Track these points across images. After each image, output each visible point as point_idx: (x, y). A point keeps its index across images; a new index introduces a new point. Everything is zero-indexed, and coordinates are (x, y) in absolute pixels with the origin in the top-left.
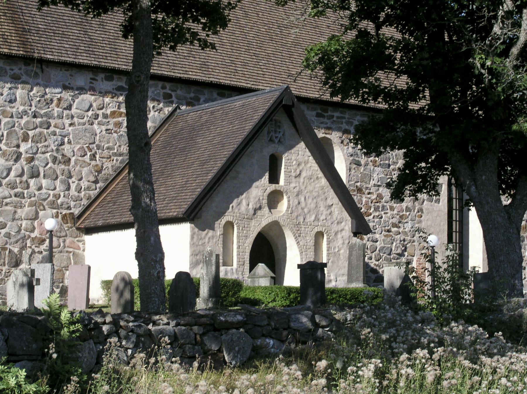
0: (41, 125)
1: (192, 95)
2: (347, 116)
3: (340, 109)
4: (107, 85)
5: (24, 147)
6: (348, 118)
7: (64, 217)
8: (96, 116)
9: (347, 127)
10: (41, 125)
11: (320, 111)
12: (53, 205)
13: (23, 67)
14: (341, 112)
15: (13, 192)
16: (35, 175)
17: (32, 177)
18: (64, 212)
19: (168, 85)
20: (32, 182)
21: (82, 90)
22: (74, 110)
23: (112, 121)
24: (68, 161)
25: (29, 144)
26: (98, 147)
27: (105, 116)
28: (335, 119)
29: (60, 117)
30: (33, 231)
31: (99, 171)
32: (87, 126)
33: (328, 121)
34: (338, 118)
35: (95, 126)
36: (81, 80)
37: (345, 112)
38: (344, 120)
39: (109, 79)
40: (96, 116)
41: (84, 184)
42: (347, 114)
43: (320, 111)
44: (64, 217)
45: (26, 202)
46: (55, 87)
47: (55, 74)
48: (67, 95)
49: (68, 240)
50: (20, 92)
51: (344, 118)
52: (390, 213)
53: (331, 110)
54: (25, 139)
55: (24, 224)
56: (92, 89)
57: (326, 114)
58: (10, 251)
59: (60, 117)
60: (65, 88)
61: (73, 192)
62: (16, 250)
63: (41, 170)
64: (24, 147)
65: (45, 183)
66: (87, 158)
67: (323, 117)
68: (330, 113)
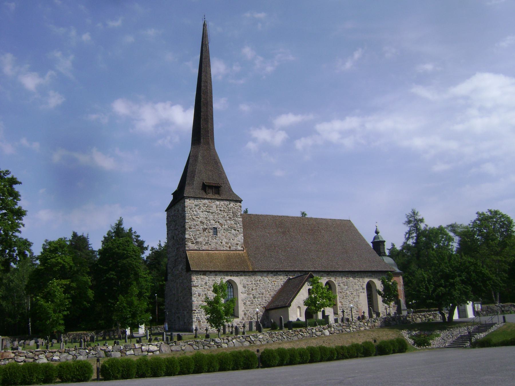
1: (293, 274)
2: (335, 274)
4: (272, 275)
11: (327, 274)
13: (251, 273)
15: (249, 303)
16: (254, 298)
18: (263, 306)
19: (287, 273)
26: (270, 290)
29: (260, 284)
32: (267, 285)
34: (333, 275)
36: (265, 274)
43: (327, 274)
52: (350, 297)
58: (251, 317)
66: (267, 293)
67: (329, 275)
68: (330, 274)
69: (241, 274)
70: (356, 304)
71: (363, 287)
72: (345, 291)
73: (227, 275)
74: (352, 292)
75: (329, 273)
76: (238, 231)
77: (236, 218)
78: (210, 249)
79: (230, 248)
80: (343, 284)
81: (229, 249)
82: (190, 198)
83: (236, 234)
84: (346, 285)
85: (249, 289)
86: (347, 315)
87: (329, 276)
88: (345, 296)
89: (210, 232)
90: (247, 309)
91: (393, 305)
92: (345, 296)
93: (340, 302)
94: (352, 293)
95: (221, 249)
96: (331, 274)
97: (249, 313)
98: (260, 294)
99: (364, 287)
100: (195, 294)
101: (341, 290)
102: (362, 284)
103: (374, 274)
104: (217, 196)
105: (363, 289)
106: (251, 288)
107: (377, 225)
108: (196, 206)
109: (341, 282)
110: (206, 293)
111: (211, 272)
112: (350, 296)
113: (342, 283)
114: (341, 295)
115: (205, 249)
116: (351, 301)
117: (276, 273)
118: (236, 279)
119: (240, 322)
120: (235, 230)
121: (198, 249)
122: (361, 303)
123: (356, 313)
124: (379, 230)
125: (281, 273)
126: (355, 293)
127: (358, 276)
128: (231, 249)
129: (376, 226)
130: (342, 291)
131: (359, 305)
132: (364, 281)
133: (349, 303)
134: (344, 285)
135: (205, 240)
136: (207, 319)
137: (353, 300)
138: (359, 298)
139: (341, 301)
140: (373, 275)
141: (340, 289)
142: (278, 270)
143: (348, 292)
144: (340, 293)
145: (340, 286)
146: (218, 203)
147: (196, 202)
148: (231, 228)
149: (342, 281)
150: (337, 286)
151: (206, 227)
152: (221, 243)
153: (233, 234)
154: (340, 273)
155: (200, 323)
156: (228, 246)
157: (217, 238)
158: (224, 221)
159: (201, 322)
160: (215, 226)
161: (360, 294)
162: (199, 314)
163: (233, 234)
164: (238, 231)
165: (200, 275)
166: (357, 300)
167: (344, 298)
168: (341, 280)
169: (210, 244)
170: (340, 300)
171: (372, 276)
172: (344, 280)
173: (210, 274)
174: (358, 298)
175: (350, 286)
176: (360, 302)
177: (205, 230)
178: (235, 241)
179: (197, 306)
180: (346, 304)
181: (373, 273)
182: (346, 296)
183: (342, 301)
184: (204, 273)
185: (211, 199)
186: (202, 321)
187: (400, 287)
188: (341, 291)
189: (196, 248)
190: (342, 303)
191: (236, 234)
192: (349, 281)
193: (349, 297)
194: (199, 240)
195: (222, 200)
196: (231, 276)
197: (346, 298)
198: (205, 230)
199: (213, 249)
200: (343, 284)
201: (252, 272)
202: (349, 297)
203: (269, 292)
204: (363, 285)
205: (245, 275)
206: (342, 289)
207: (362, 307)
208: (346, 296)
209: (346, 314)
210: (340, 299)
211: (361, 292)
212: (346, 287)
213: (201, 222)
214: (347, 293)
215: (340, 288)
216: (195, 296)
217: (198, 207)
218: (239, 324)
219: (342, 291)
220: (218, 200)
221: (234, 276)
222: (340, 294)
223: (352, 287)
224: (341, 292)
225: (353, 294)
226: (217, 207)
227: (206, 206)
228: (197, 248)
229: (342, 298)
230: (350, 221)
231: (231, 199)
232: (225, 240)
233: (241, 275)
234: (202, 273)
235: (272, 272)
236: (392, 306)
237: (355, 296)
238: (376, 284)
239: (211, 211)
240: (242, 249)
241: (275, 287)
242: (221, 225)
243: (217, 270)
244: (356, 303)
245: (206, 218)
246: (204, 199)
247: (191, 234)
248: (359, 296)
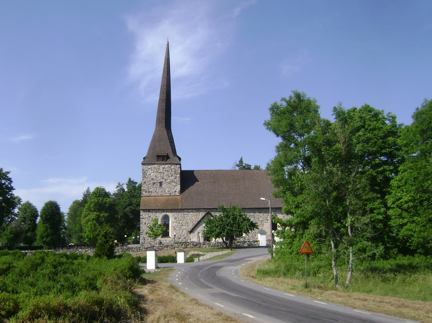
0: (183, 218)
4: (195, 211)
5: (181, 222)
7: (188, 231)
8: (193, 216)
10: (183, 218)
12: (186, 230)
16: (182, 225)
17: (182, 226)
20: (182, 227)
21: (190, 212)
22: (189, 215)
23: (196, 216)
24: (188, 223)
25: (181, 221)
27: (194, 216)
29: (187, 217)
30: (182, 234)
31: (194, 224)
35: (193, 217)
36: (190, 211)
39: (195, 210)
40: (193, 216)
41: (191, 226)
44: (188, 231)
45: (181, 230)
46: (186, 212)
47: (185, 210)
48: (188, 213)
49: (188, 235)
50: (180, 214)
54: (181, 220)
55: (181, 233)
56: (192, 212)
59: (187, 217)
60: (187, 212)
61: (189, 227)
62: (179, 237)
63: (184, 225)
64: (181, 222)
65: (184, 227)
66: (191, 222)
69: (173, 210)
71: (268, 219)
73: (164, 212)
76: (177, 183)
77: (175, 175)
78: (157, 195)
79: (170, 194)
81: (169, 195)
82: (146, 165)
83: (176, 186)
85: (178, 220)
89: (158, 185)
90: (177, 232)
95: (164, 195)
97: (178, 235)
98: (186, 223)
100: (143, 223)
102: (266, 217)
103: (278, 210)
104: (163, 162)
105: (268, 220)
106: (180, 220)
108: (149, 169)
110: (149, 222)
111: (153, 210)
115: (154, 195)
117: (198, 210)
118: (170, 215)
119: (171, 240)
120: (175, 183)
121: (149, 196)
125: (202, 210)
127: (264, 211)
128: (172, 195)
135: (153, 190)
136: (161, 237)
140: (277, 211)
142: (199, 208)
146: (163, 166)
147: (149, 167)
148: (172, 182)
151: (155, 181)
152: (165, 191)
153: (174, 186)
155: (145, 241)
156: (169, 193)
157: (162, 189)
158: (168, 178)
159: (146, 240)
160: (161, 181)
162: (144, 235)
163: (174, 186)
164: (177, 183)
165: (146, 211)
169: (157, 192)
171: (276, 211)
173: (153, 211)
177: (154, 183)
178: (174, 190)
179: (143, 230)
184: (149, 211)
185: (159, 164)
186: (146, 239)
189: (148, 195)
191: (176, 186)
194: (150, 190)
195: (167, 164)
196: (166, 212)
198: (154, 183)
199: (159, 195)
201: (181, 209)
203: (192, 222)
204: (267, 217)
205: (176, 212)
209: (251, 237)
211: (266, 222)
213: (153, 179)
216: (142, 224)
217: (151, 170)
218: (171, 242)
220: (164, 164)
221: (168, 212)
226: (163, 169)
227: (156, 168)
228: (149, 195)
231: (173, 163)
232: (168, 189)
233: (174, 212)
234: (147, 211)
235: (195, 209)
239: (159, 172)
240: (179, 194)
241: (197, 219)
242: (165, 180)
243: (157, 208)
245: (156, 176)
246: (155, 164)
247: (146, 186)
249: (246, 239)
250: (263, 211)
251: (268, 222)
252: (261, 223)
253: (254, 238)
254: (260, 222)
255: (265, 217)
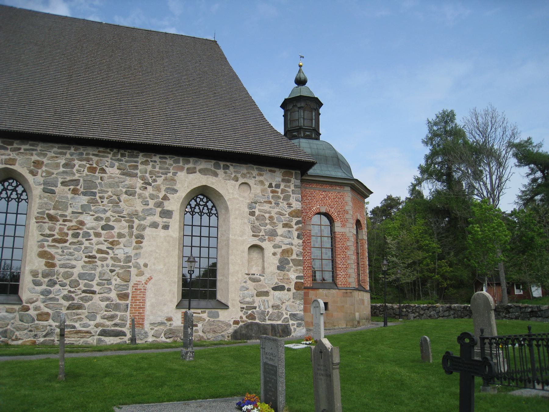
2: (39, 148)
3: (30, 142)
6: (40, 150)
9: (38, 159)
14: (31, 145)
28: (22, 151)
33: (11, 153)
34: (25, 150)
37: (38, 145)
38: (34, 152)
42: (40, 146)
51: (36, 150)
52: (95, 240)
53: (16, 144)
57: (9, 147)
67: (7, 149)
68: (15, 146)
70: (122, 267)
71: (168, 206)
72: (73, 213)
74: (108, 219)
75: (12, 144)
80: (72, 187)
84: (84, 194)
86: (68, 308)
87: (9, 152)
88: (70, 232)
91: (296, 283)
92: (70, 232)
93: (43, 255)
94: (111, 223)
96: (20, 149)
99: (169, 208)
101: (55, 208)
102: (161, 195)
105: (167, 214)
107: (301, 64)
109: (60, 180)
112: (97, 235)
113: (63, 183)
114: (51, 229)
116: (98, 255)
122: (146, 265)
123: (118, 301)
124: (307, 74)
126: (121, 227)
129: (300, 66)
130: (60, 212)
131: (133, 271)
132: (175, 187)
133: (87, 260)
134: (75, 192)
137: (108, 253)
138: (142, 248)
139: (46, 249)
140: (220, 172)
141: (52, 207)
143: (89, 220)
144: (47, 220)
145: (53, 192)
149: (68, 178)
150: (37, 191)
154: (59, 148)
161: (148, 232)
166: (130, 251)
167: (66, 241)
168: (64, 172)
170: (42, 246)
171: (216, 175)
172: (76, 177)
174: (134, 244)
175: (101, 198)
176: (141, 262)
180: (74, 263)
181: (222, 164)
182: (76, 235)
183: (52, 251)
187: (343, 226)
188: (52, 212)
190: (53, 257)
192: (101, 178)
193: (92, 237)
197: (75, 240)
200: (72, 187)
202: (92, 237)
204: (165, 198)
206: (61, 205)
207: (150, 279)
208: (76, 235)
209: (62, 301)
210: (46, 244)
211: (154, 225)
212: (84, 200)
214: (82, 223)
215: (50, 199)
219: (60, 212)
222: (50, 224)
223: (116, 204)
224: (51, 218)
225: (112, 228)
229: (55, 241)
230: (216, 42)
236: (293, 284)
237: (120, 235)
238: (228, 203)
244: (122, 264)
248: (140, 239)
249: (32, 312)
250: (145, 163)
251: (166, 227)
252: (131, 227)
253: (79, 307)
254: (124, 224)
255: (152, 197)
